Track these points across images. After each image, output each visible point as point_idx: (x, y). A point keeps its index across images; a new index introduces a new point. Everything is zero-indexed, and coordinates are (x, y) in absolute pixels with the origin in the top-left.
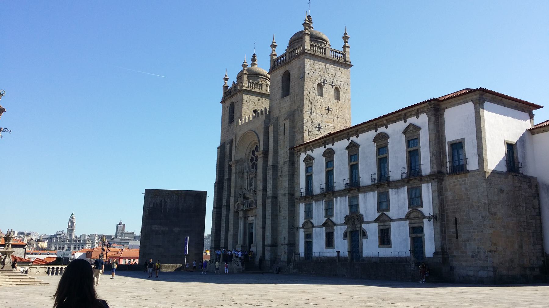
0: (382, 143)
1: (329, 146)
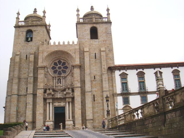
0: (177, 74)
1: (141, 70)
